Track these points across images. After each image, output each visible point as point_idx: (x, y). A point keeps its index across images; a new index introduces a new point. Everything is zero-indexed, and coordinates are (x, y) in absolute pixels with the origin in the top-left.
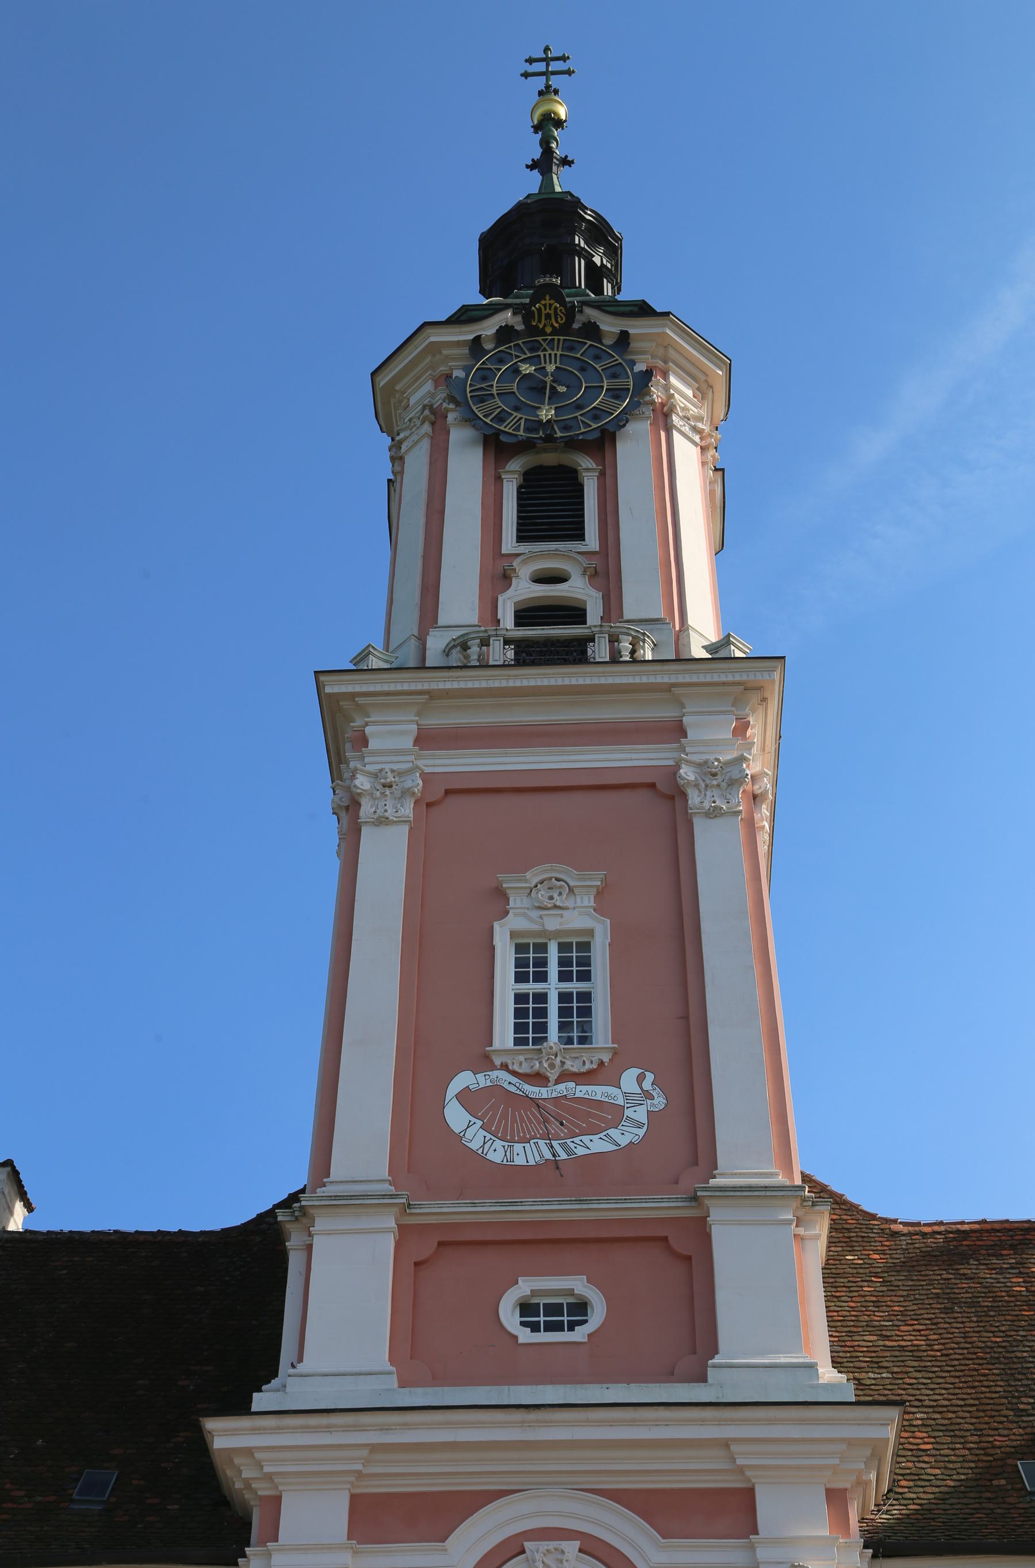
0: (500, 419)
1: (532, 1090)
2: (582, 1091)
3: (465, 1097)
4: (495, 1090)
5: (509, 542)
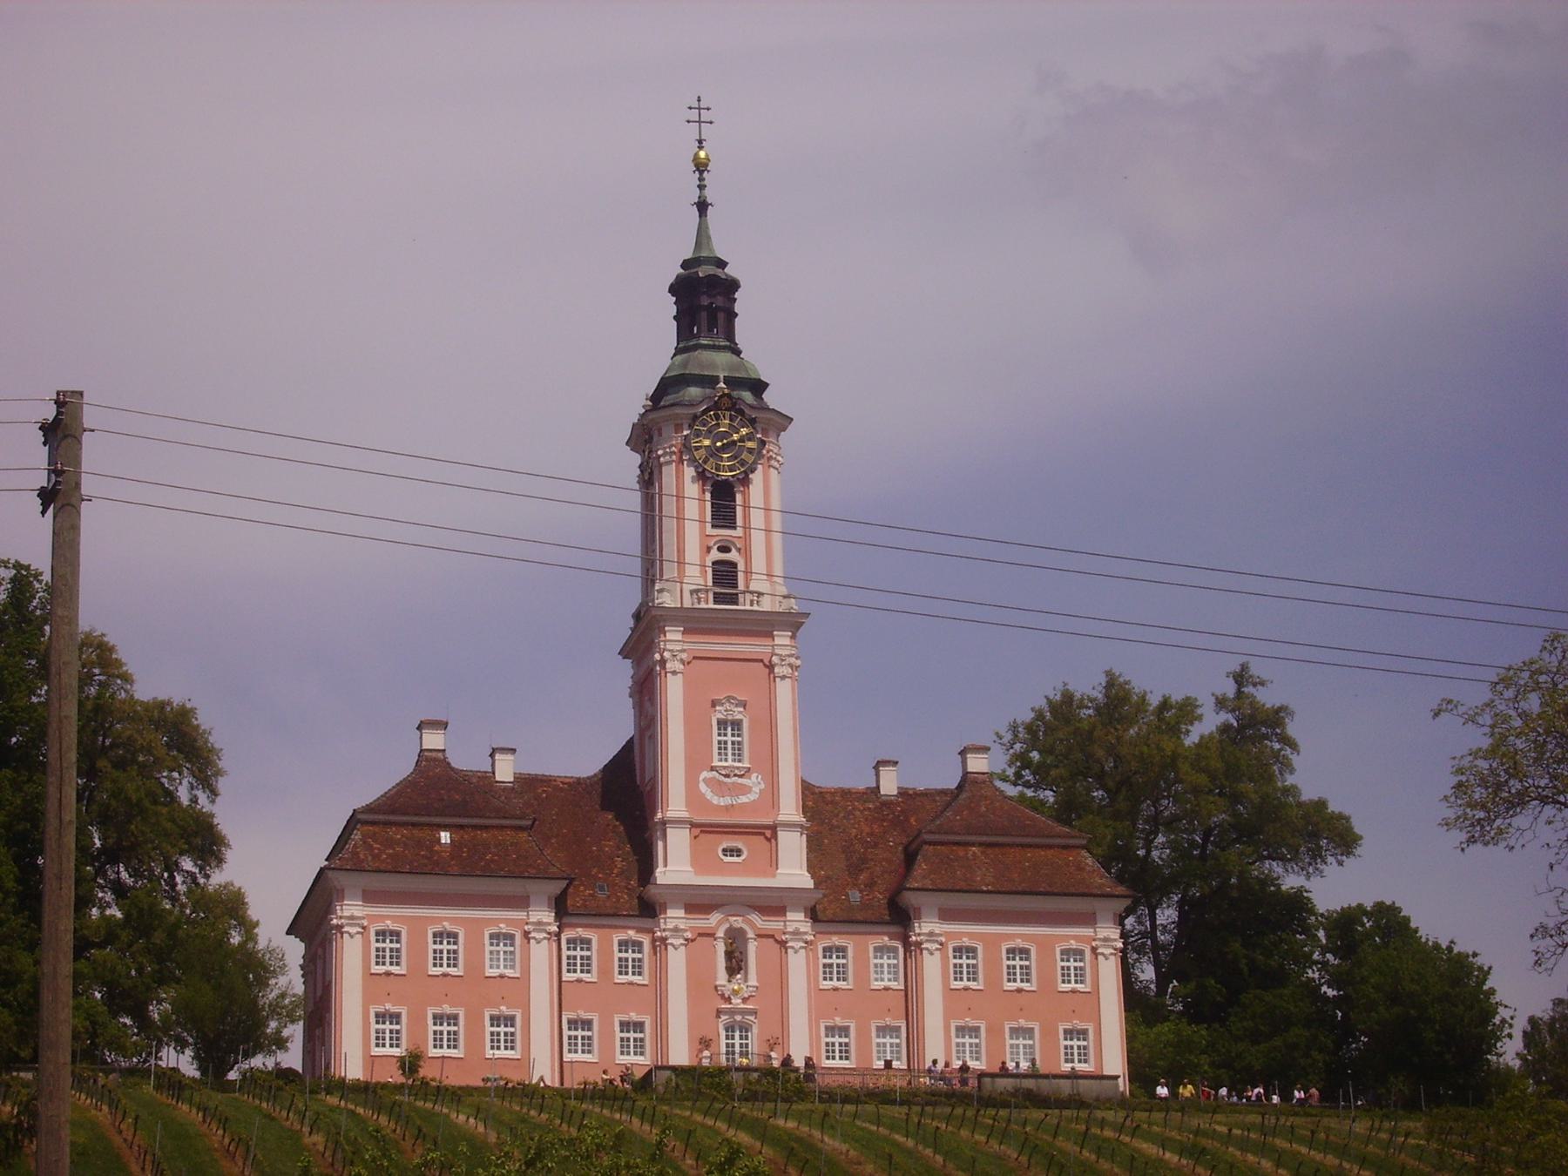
0: (705, 462)
1: (727, 780)
2: (740, 780)
4: (714, 778)
5: (709, 530)
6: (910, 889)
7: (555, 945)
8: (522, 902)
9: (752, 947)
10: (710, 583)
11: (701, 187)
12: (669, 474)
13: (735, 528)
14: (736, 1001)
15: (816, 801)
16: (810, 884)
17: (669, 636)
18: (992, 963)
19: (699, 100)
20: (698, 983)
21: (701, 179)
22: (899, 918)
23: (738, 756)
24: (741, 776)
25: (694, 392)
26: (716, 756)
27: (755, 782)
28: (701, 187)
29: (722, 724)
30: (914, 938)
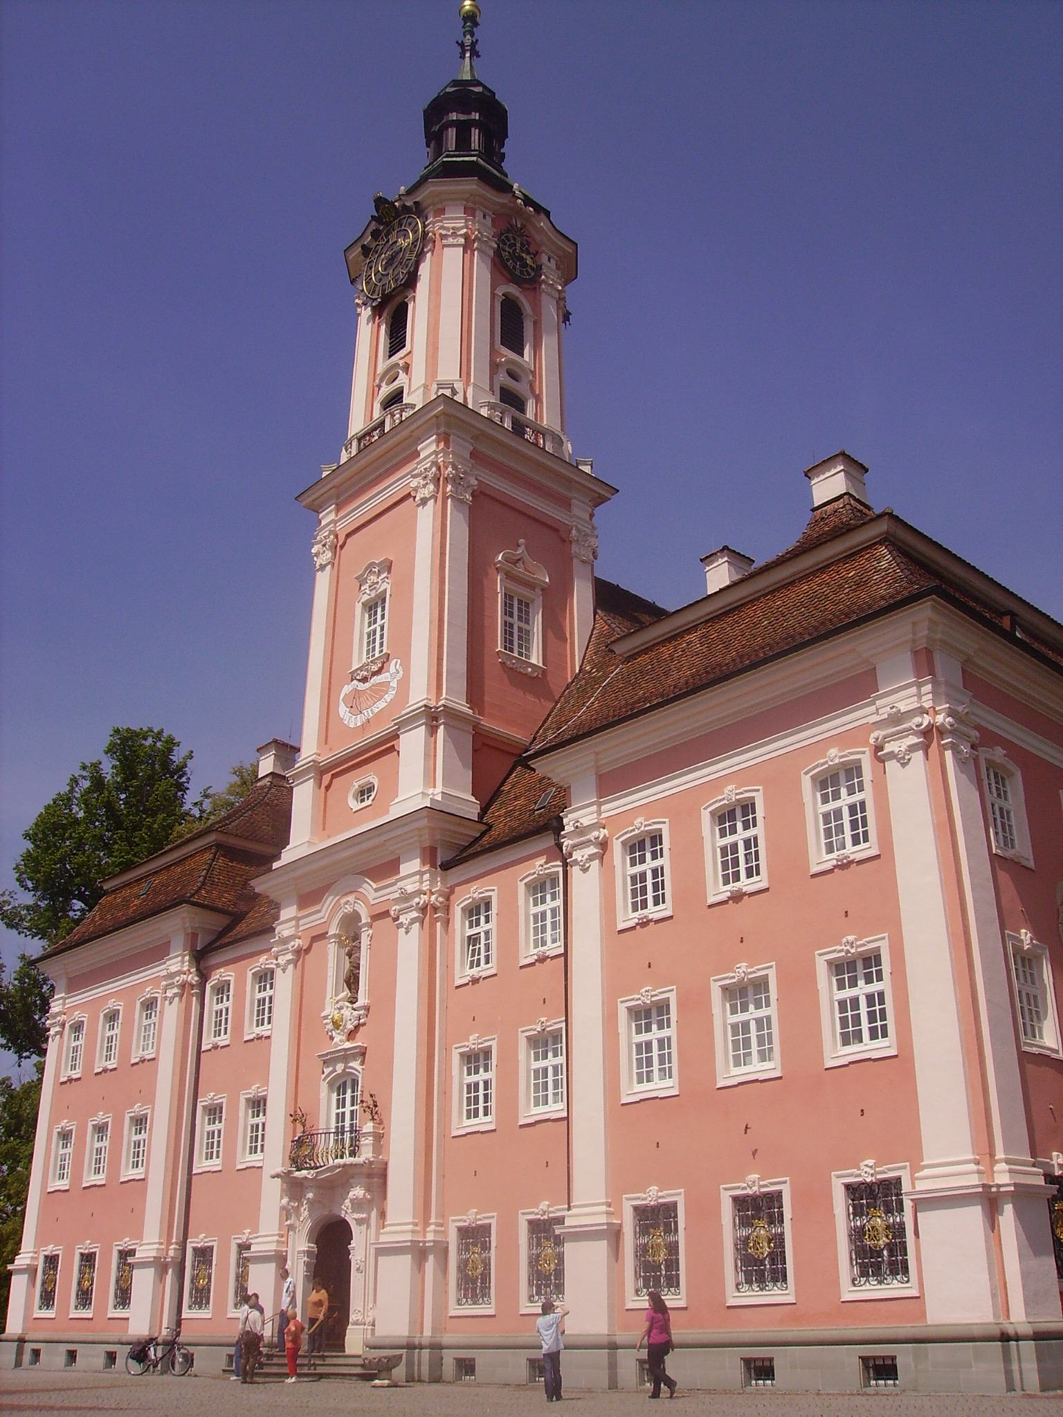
24: (379, 672)
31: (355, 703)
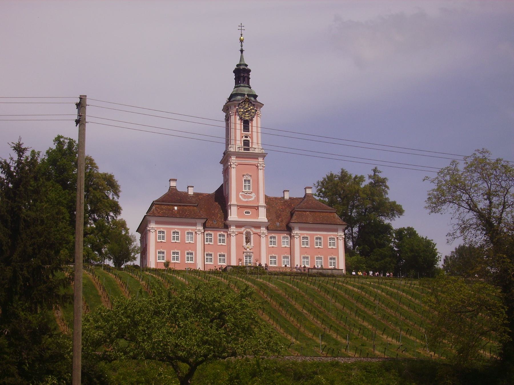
0: (242, 115)
1: (246, 195)
2: (250, 195)
3: (241, 195)
5: (243, 132)
6: (291, 222)
7: (203, 235)
8: (195, 225)
9: (252, 236)
10: (243, 145)
11: (242, 46)
12: (233, 118)
13: (249, 132)
14: (248, 250)
15: (269, 200)
16: (267, 221)
17: (232, 159)
18: (312, 241)
19: (241, 24)
20: (239, 245)
21: (241, 44)
22: (289, 229)
23: (249, 189)
24: (250, 194)
25: (239, 97)
26: (244, 189)
27: (253, 195)
28: (242, 46)
29: (245, 181)
30: (292, 235)
31: (244, 197)
